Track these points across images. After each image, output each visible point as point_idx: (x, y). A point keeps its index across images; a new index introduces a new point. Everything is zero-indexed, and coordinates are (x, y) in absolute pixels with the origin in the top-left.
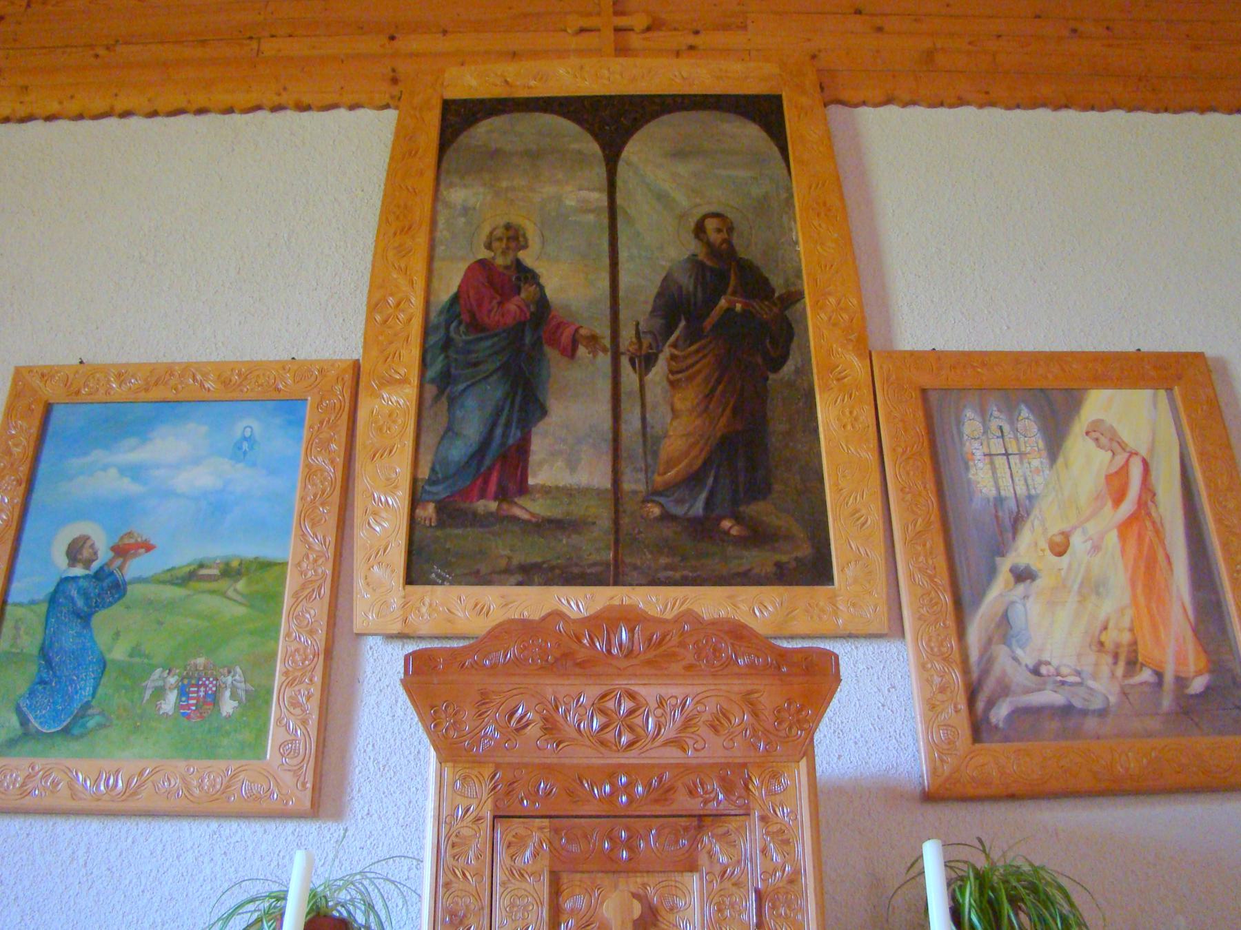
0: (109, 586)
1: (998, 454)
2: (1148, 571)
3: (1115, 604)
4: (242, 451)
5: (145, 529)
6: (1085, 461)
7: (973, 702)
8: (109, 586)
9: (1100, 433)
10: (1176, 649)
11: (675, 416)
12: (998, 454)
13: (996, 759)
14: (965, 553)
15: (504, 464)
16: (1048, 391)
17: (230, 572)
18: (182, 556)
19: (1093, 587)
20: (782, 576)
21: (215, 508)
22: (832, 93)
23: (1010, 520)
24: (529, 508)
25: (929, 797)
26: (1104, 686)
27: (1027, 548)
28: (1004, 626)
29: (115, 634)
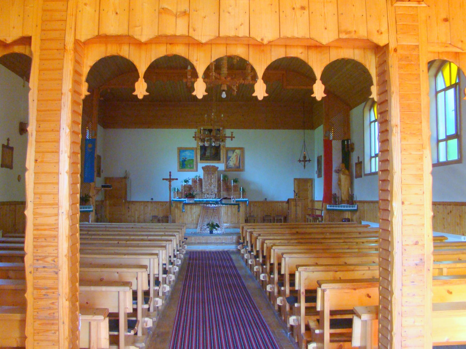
0: (185, 160)
1: (230, 154)
2: (237, 161)
3: (235, 162)
4: (191, 153)
5: (186, 157)
6: (235, 154)
7: (227, 167)
8: (185, 160)
9: (236, 153)
10: (237, 165)
11: (213, 151)
12: (230, 154)
13: (227, 170)
14: (228, 159)
15: (205, 154)
16: (233, 150)
17: (191, 160)
18: (189, 158)
19: (233, 161)
20: (218, 160)
21: (190, 156)
22: (224, 128)
23: (230, 157)
24: (206, 156)
25: (225, 171)
26: (233, 166)
27: (231, 159)
28: (229, 163)
29: (186, 163)
